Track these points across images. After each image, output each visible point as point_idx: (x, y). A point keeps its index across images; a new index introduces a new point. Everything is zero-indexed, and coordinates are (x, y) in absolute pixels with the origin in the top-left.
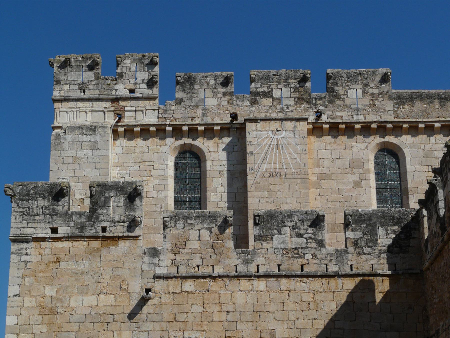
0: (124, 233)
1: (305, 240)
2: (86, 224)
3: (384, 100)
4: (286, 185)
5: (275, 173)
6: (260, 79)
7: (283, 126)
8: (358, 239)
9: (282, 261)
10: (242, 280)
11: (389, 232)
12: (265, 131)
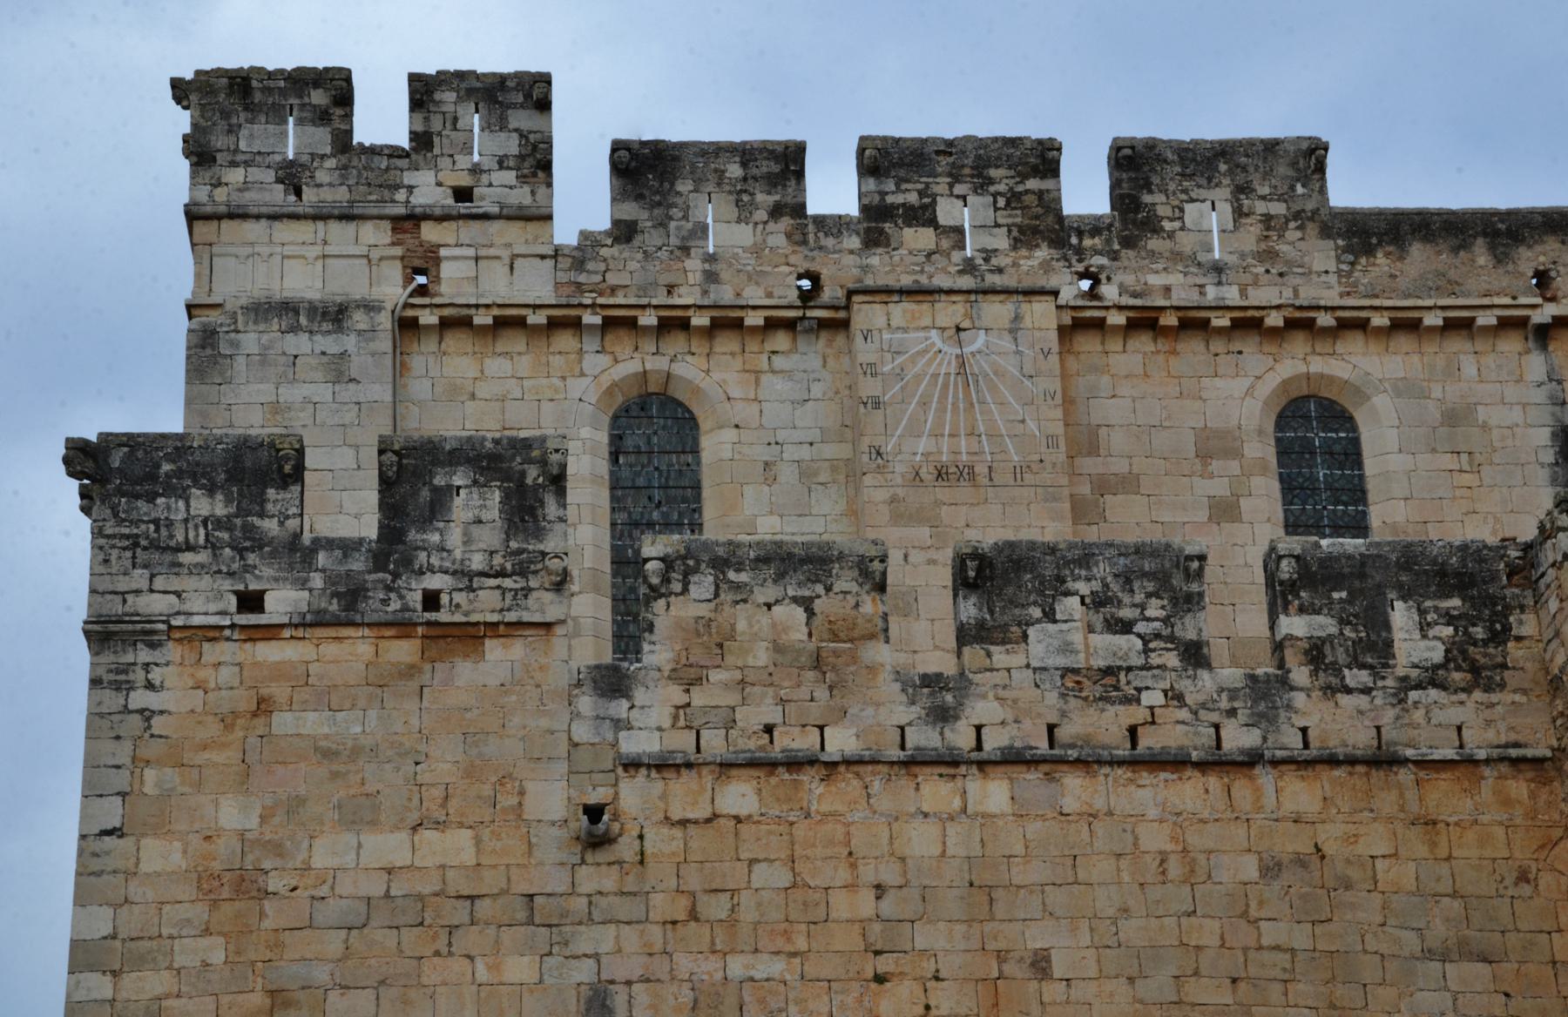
1: (1139, 644)
2: (366, 581)
3: (1307, 237)
6: (894, 165)
7: (975, 316)
8: (1323, 641)
9: (1063, 714)
10: (924, 773)
11: (1429, 619)
12: (918, 329)
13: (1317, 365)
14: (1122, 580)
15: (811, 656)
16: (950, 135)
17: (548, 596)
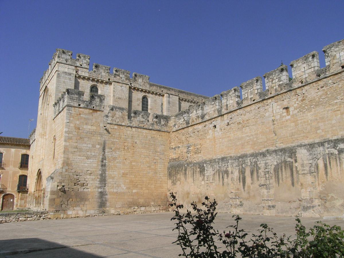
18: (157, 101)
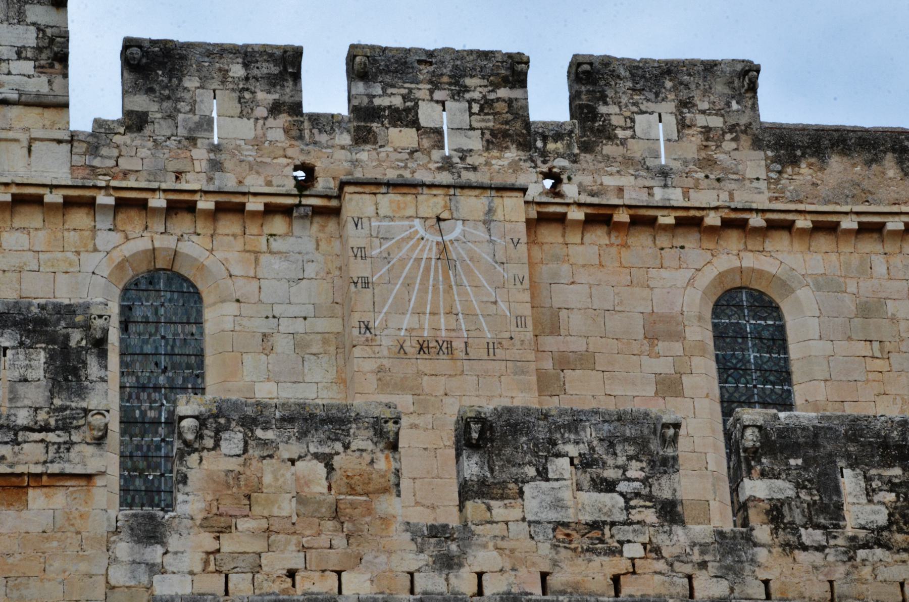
0: (48, 465)
1: (621, 501)
3: (741, 148)
4: (466, 377)
5: (437, 341)
7: (453, 208)
8: (782, 502)
9: (555, 563)
11: (874, 486)
13: (750, 261)
14: (606, 444)
15: (330, 507)
16: (430, 47)
17: (90, 450)
18: (891, 307)
